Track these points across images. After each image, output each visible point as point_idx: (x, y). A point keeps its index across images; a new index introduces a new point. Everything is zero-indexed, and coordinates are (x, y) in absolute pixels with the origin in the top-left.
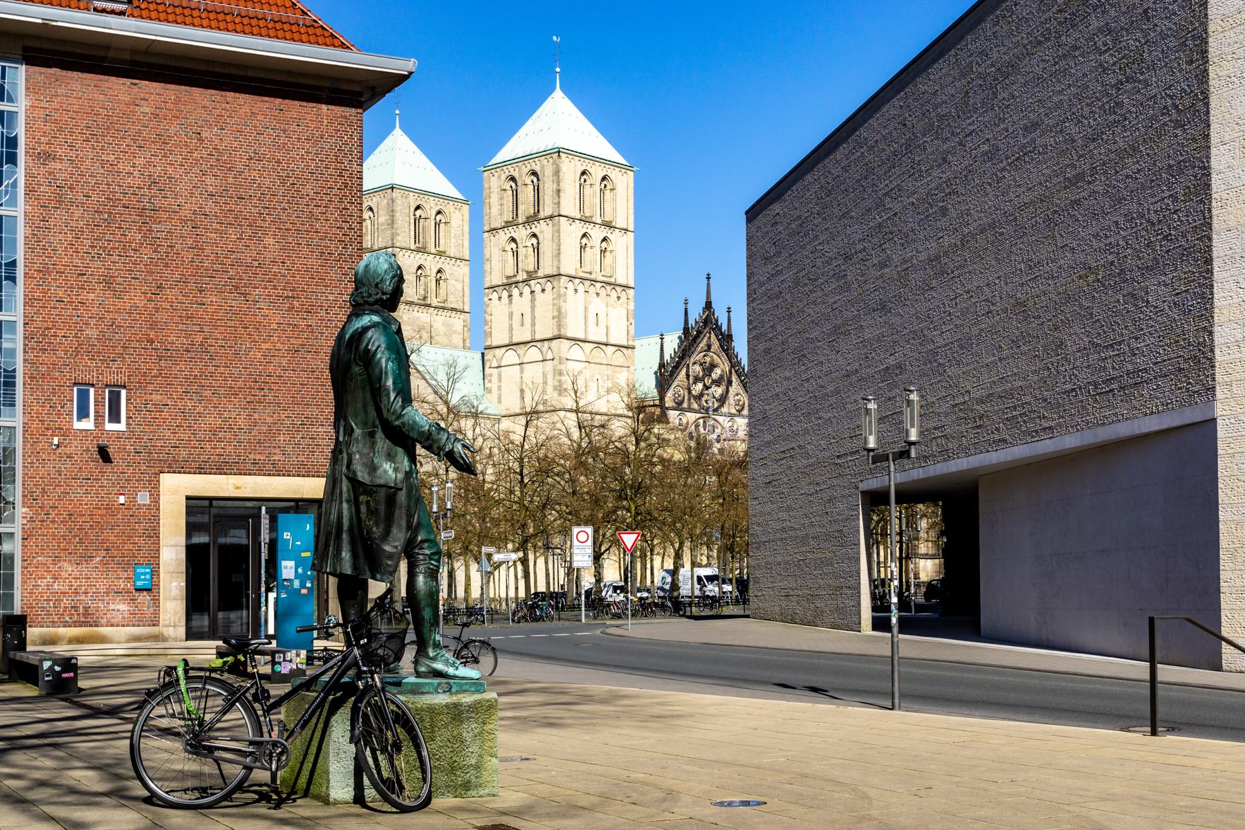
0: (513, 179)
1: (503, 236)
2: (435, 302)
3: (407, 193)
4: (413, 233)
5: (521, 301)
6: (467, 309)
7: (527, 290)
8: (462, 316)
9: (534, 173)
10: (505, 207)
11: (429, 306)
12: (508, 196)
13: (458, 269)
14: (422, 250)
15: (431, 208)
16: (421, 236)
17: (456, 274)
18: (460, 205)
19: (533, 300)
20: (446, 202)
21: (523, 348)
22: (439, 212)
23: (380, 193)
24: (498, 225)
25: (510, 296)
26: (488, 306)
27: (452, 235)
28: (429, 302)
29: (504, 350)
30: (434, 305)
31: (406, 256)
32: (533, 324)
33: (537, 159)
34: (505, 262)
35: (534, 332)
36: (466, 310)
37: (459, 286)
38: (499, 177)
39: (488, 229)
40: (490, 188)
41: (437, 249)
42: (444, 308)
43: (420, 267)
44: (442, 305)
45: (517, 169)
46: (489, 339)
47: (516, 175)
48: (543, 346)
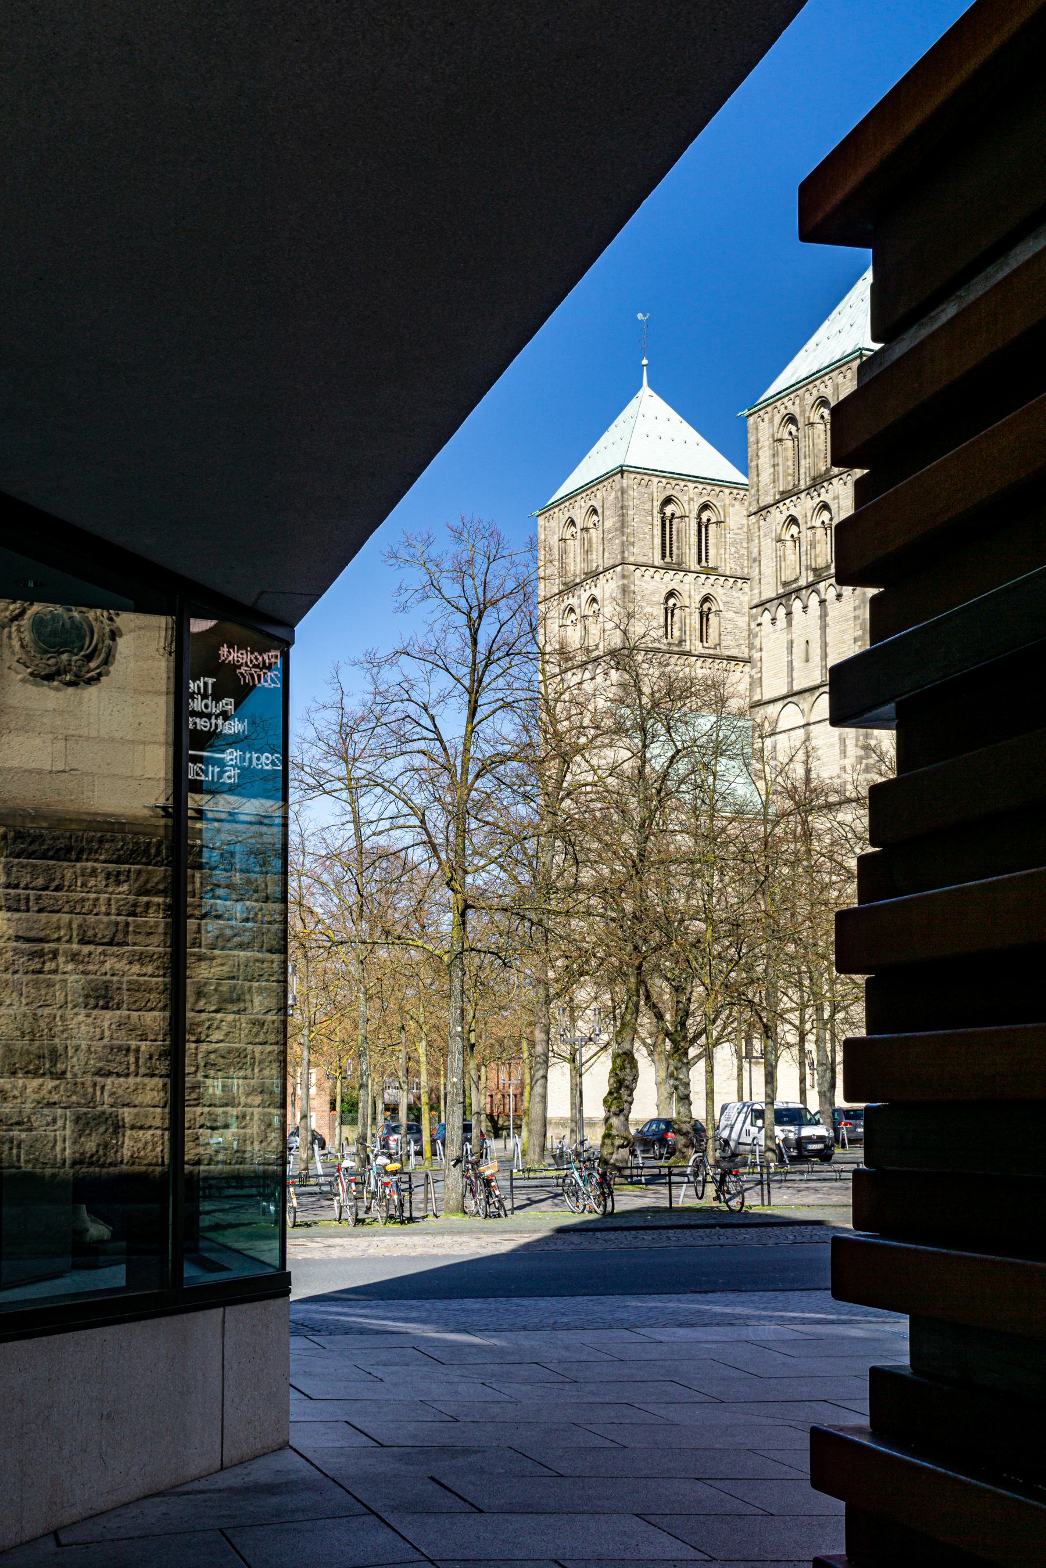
0: (792, 419)
1: (778, 517)
4: (658, 541)
7: (814, 600)
10: (780, 468)
12: (786, 449)
13: (740, 593)
15: (691, 499)
16: (675, 545)
17: (737, 603)
19: (824, 615)
20: (718, 489)
22: (705, 507)
23: (606, 483)
24: (770, 500)
25: (789, 614)
26: (756, 636)
29: (780, 704)
30: (696, 653)
34: (780, 559)
38: (771, 420)
39: (755, 510)
40: (758, 442)
43: (671, 594)
44: (711, 652)
45: (797, 402)
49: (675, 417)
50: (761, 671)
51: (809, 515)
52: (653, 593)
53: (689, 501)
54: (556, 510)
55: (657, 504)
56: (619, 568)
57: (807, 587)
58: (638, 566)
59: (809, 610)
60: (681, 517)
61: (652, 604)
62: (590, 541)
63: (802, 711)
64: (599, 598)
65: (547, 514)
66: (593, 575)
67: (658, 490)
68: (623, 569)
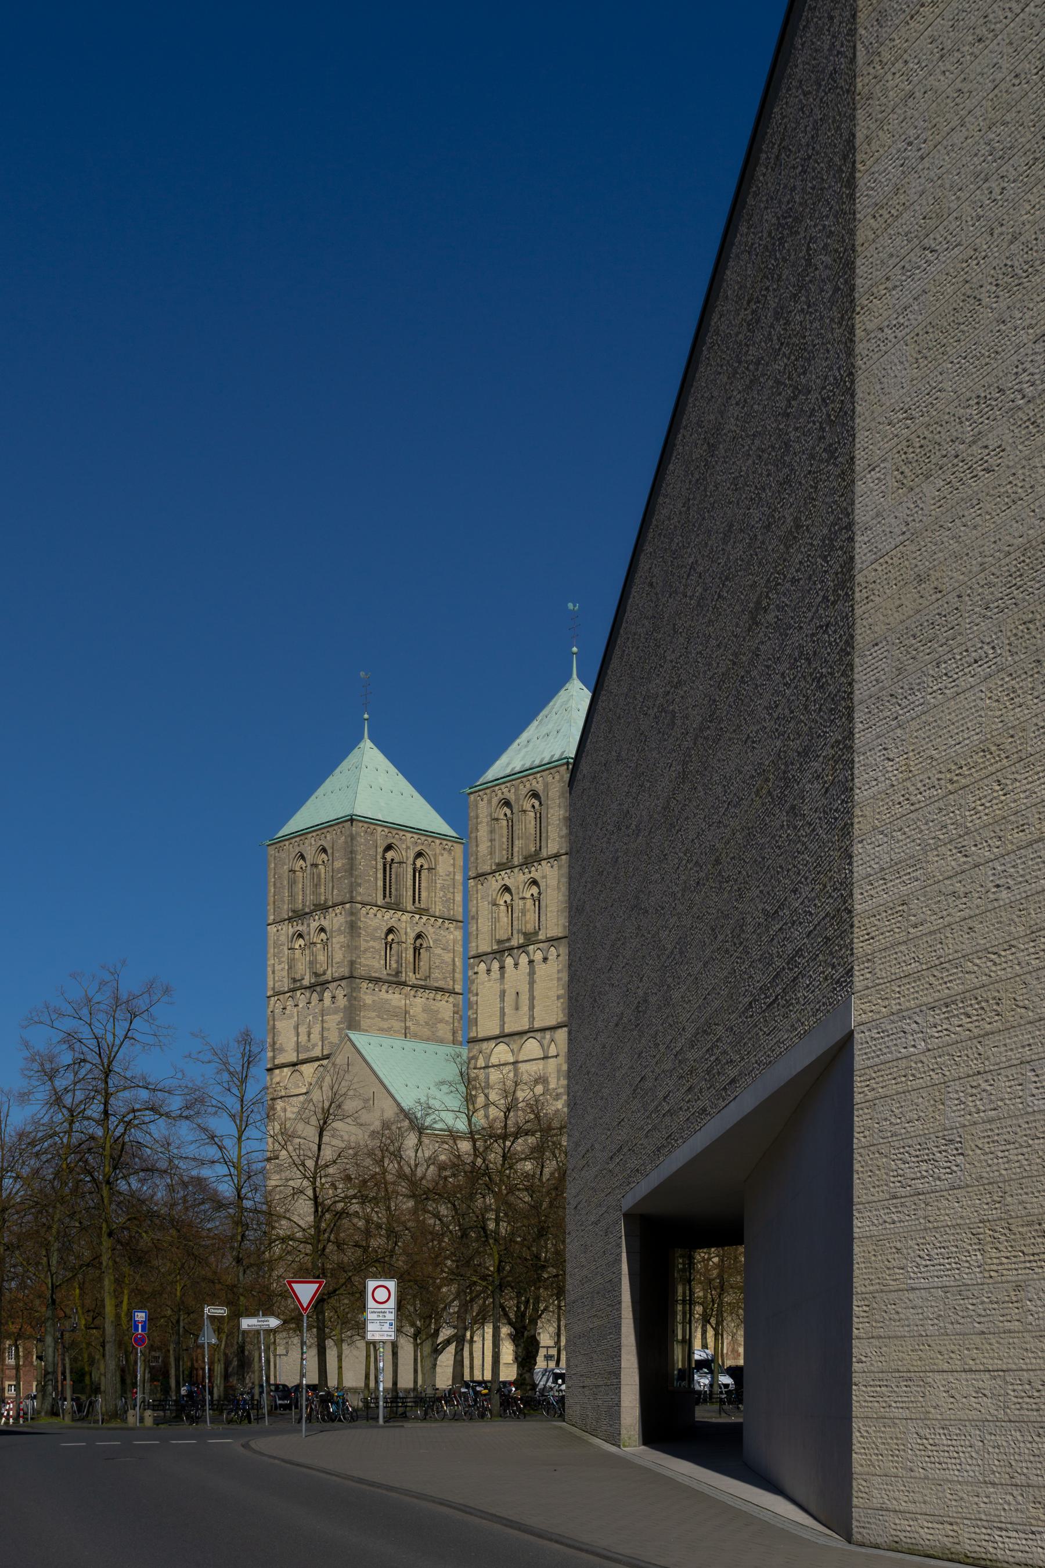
0: (507, 804)
1: (494, 884)
2: (412, 979)
3: (373, 827)
4: (380, 883)
5: (516, 974)
6: (458, 988)
7: (524, 960)
8: (451, 999)
9: (535, 795)
10: (497, 844)
11: (404, 984)
12: (501, 827)
13: (446, 933)
14: (395, 906)
15: (408, 848)
16: (393, 887)
17: (444, 941)
18: (450, 844)
19: (532, 973)
20: (430, 839)
21: (519, 1041)
22: (419, 855)
23: (336, 827)
24: (487, 868)
25: (502, 968)
26: (473, 982)
27: (438, 886)
28: (403, 979)
29: (492, 1044)
31: (371, 915)
32: (532, 1007)
33: (539, 775)
34: (495, 920)
35: (532, 1018)
36: (457, 990)
37: (447, 957)
38: (490, 801)
39: (474, 875)
41: (417, 905)
42: (424, 988)
43: (390, 931)
45: (513, 791)
46: (474, 1028)
47: (511, 797)
48: (544, 1038)
49: (393, 770)
50: (476, 1013)
51: (521, 887)
52: (376, 929)
53: (406, 852)
54: (287, 843)
55: (380, 850)
56: (348, 906)
57: (518, 948)
58: (364, 904)
59: (519, 967)
60: (400, 863)
61: (374, 939)
62: (319, 875)
63: (512, 1051)
64: (328, 929)
65: (278, 845)
66: (323, 908)
67: (381, 838)
68: (351, 907)
